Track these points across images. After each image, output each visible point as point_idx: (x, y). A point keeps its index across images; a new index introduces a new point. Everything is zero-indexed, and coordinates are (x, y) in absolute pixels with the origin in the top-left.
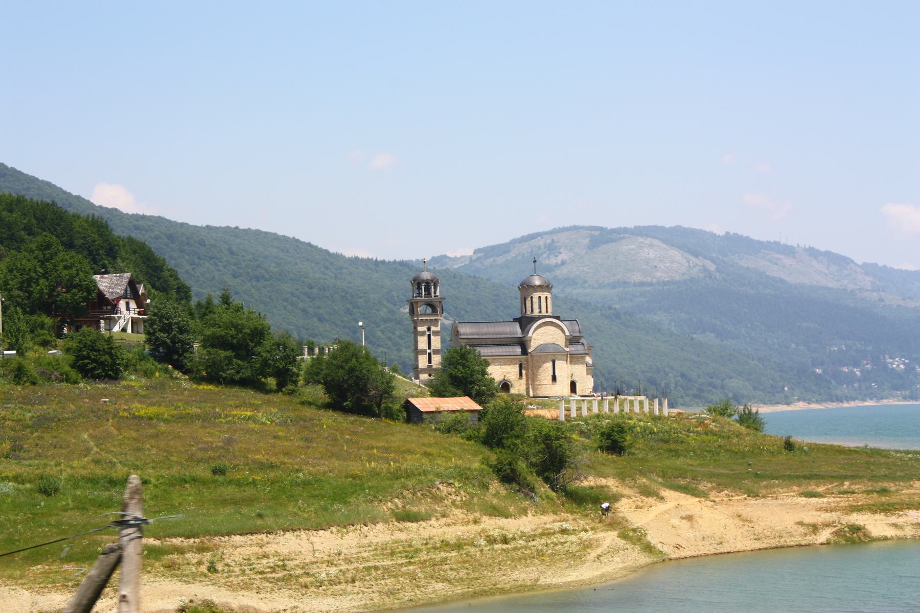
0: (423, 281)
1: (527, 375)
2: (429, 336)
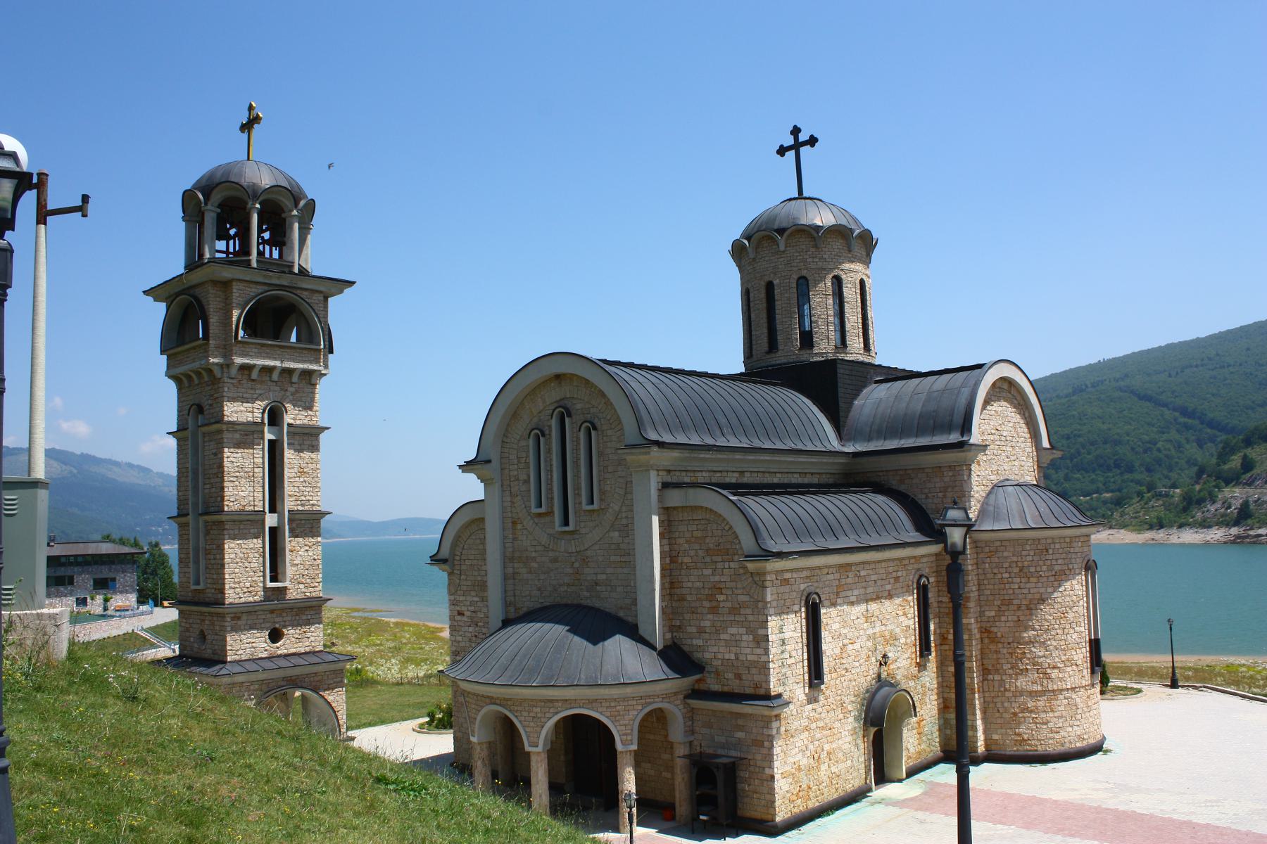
0: (254, 192)
2: (275, 451)
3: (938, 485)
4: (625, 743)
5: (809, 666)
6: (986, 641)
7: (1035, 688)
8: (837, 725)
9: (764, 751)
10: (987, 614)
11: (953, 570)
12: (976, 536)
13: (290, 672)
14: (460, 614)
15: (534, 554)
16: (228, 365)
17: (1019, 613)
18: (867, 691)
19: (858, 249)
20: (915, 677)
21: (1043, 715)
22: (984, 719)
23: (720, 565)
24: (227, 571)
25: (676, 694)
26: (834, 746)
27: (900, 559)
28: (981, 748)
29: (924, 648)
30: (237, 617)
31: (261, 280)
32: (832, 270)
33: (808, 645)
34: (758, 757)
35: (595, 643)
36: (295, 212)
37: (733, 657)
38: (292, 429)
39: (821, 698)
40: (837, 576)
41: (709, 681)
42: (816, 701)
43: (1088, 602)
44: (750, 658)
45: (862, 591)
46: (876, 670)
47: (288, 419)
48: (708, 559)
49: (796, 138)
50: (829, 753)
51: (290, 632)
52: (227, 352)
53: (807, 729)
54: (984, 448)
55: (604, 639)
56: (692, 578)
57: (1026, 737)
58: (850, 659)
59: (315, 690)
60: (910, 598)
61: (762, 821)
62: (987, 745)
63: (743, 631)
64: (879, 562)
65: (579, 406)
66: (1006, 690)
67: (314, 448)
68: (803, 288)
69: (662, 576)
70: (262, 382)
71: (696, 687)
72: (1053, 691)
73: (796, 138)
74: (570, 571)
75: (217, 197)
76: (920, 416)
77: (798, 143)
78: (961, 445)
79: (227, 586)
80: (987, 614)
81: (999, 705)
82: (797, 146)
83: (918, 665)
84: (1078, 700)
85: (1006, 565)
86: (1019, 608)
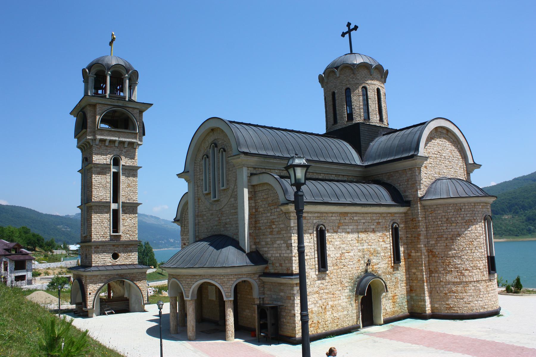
0: (109, 68)
1: (408, 256)
2: (116, 177)
3: (405, 178)
4: (228, 297)
5: (318, 261)
6: (431, 256)
7: (456, 280)
8: (338, 292)
9: (291, 302)
10: (431, 242)
11: (411, 221)
12: (423, 202)
13: (120, 272)
14: (185, 244)
15: (205, 213)
16: (95, 139)
17: (447, 241)
18: (358, 278)
19: (376, 74)
20: (390, 273)
21: (461, 295)
22: (430, 296)
23: (273, 211)
24: (93, 227)
25: (254, 274)
26: (336, 303)
27: (381, 214)
28: (428, 310)
29: (397, 258)
30: (97, 247)
31: (109, 103)
32: (362, 84)
33: (318, 251)
34: (289, 305)
35: (218, 249)
36: (127, 75)
37: (279, 255)
38: (124, 167)
39: (327, 278)
40: (338, 218)
41: (270, 268)
42: (323, 279)
43: (486, 237)
44: (285, 255)
45: (355, 227)
46: (364, 267)
47: (122, 163)
48: (269, 208)
49: (349, 28)
50: (332, 307)
51: (122, 255)
52: (94, 134)
53: (317, 292)
54: (426, 158)
55: (223, 248)
56: (263, 218)
57: (452, 306)
58: (346, 261)
59: (132, 281)
60: (387, 234)
61: (290, 337)
62: (432, 310)
63: (282, 242)
64: (366, 213)
65: (220, 142)
66: (441, 281)
67: (135, 176)
68: (348, 92)
69: (250, 218)
70: (111, 147)
71: (265, 271)
72: (466, 282)
73: (349, 28)
74: (217, 219)
75: (94, 71)
76: (397, 146)
77: (351, 29)
78: (412, 156)
79: (93, 234)
80: (431, 242)
81: (438, 289)
82: (349, 32)
83: (393, 267)
84: (481, 287)
85: (439, 217)
86: (447, 239)
